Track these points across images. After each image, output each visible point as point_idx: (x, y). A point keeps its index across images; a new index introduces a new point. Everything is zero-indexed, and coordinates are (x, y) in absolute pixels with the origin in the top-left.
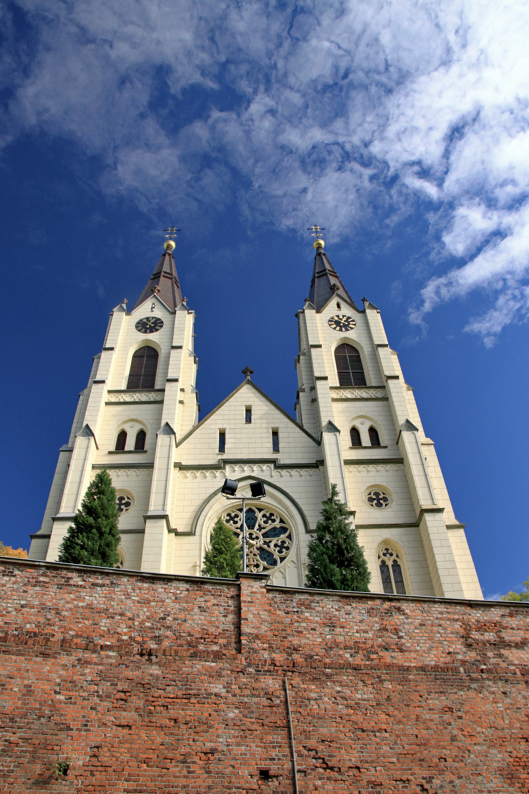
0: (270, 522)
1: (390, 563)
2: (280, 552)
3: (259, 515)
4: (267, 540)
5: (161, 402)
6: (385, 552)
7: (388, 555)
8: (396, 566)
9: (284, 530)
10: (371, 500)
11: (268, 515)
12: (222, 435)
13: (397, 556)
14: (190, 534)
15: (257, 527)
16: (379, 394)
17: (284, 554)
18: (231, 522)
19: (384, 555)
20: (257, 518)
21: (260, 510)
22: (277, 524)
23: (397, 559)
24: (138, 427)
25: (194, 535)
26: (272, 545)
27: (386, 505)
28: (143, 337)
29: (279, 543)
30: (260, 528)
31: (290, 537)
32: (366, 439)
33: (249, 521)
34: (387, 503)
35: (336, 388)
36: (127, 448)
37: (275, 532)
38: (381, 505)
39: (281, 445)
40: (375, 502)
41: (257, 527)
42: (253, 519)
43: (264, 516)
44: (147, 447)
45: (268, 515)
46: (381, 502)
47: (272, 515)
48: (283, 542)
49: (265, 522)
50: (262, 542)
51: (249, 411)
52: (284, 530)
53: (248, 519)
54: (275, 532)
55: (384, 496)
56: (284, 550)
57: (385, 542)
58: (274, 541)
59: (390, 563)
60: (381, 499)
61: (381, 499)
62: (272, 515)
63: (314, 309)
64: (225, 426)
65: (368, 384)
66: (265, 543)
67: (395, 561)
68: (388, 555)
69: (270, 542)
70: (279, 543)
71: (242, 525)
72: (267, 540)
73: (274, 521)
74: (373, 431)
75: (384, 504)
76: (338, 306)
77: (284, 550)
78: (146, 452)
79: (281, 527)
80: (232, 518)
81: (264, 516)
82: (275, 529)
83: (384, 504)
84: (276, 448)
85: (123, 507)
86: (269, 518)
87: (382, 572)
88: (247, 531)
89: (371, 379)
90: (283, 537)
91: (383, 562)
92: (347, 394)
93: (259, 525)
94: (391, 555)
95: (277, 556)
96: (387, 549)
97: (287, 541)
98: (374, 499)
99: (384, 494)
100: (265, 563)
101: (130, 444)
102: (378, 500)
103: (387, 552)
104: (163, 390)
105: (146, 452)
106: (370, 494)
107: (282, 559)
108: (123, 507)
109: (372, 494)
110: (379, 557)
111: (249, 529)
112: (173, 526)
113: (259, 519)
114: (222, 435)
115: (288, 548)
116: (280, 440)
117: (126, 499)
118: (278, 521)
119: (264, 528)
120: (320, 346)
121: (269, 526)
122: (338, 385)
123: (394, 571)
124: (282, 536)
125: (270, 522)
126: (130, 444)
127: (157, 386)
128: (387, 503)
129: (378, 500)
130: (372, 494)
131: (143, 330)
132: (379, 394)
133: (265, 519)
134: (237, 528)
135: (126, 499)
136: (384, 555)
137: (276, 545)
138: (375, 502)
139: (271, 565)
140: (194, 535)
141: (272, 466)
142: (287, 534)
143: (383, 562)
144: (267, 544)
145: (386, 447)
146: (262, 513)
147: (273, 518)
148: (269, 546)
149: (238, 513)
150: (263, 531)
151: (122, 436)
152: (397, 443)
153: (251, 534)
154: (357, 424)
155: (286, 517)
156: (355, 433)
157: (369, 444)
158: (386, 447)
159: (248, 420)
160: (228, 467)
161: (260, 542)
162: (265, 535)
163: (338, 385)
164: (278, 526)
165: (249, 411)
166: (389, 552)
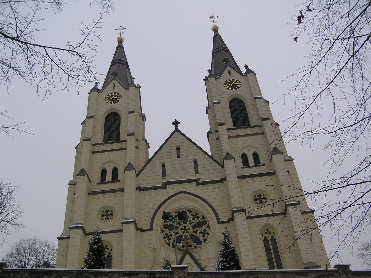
0: (196, 218)
1: (269, 238)
2: (203, 236)
4: (195, 230)
5: (125, 149)
6: (266, 231)
7: (268, 233)
8: (273, 240)
9: (205, 223)
10: (256, 200)
11: (195, 214)
12: (163, 166)
13: (274, 233)
14: (151, 229)
15: (188, 222)
16: (258, 130)
19: (266, 233)
20: (188, 216)
22: (201, 220)
23: (273, 235)
24: (113, 166)
25: (152, 230)
26: (198, 232)
29: (203, 231)
31: (208, 227)
34: (266, 201)
35: (231, 129)
37: (199, 225)
38: (263, 202)
39: (199, 170)
40: (259, 200)
43: (192, 215)
44: (119, 178)
45: (195, 214)
46: (263, 200)
47: (197, 214)
48: (205, 230)
49: (193, 219)
50: (192, 231)
51: (178, 149)
54: (199, 225)
55: (264, 196)
56: (206, 235)
57: (267, 225)
58: (200, 230)
59: (269, 238)
60: (262, 199)
61: (262, 199)
64: (164, 161)
65: (252, 125)
66: (194, 231)
67: (272, 237)
68: (268, 233)
69: (197, 231)
70: (203, 231)
72: (195, 230)
73: (198, 218)
74: (256, 156)
75: (264, 202)
77: (206, 235)
78: (119, 181)
79: (203, 221)
81: (192, 215)
82: (199, 222)
83: (264, 202)
84: (197, 171)
85: (109, 216)
87: (265, 244)
89: (253, 121)
90: (204, 227)
91: (265, 238)
92: (240, 132)
93: (190, 221)
94: (270, 233)
95: (201, 239)
96: (267, 230)
97: (207, 229)
98: (258, 199)
99: (264, 195)
102: (261, 199)
103: (267, 231)
104: (125, 141)
105: (119, 181)
106: (255, 196)
107: (205, 241)
108: (109, 216)
109: (257, 196)
110: (263, 235)
112: (139, 227)
113: (189, 217)
114: (163, 166)
115: (208, 234)
116: (199, 167)
118: (201, 217)
121: (196, 221)
122: (233, 127)
123: (272, 243)
125: (196, 218)
127: (122, 139)
128: (266, 201)
129: (261, 199)
130: (257, 196)
132: (258, 130)
136: (266, 233)
137: (201, 233)
138: (259, 200)
139: (199, 245)
140: (152, 230)
141: (195, 183)
142: (207, 225)
143: (265, 238)
144: (195, 232)
145: (264, 165)
146: (191, 213)
147: (198, 216)
148: (196, 233)
151: (104, 172)
152: (271, 162)
153: (185, 227)
154: (245, 151)
155: (206, 214)
156: (244, 157)
157: (253, 164)
158: (264, 165)
159: (179, 155)
160: (168, 186)
161: (191, 231)
162: (194, 227)
163: (233, 127)
165: (178, 149)
166: (269, 231)
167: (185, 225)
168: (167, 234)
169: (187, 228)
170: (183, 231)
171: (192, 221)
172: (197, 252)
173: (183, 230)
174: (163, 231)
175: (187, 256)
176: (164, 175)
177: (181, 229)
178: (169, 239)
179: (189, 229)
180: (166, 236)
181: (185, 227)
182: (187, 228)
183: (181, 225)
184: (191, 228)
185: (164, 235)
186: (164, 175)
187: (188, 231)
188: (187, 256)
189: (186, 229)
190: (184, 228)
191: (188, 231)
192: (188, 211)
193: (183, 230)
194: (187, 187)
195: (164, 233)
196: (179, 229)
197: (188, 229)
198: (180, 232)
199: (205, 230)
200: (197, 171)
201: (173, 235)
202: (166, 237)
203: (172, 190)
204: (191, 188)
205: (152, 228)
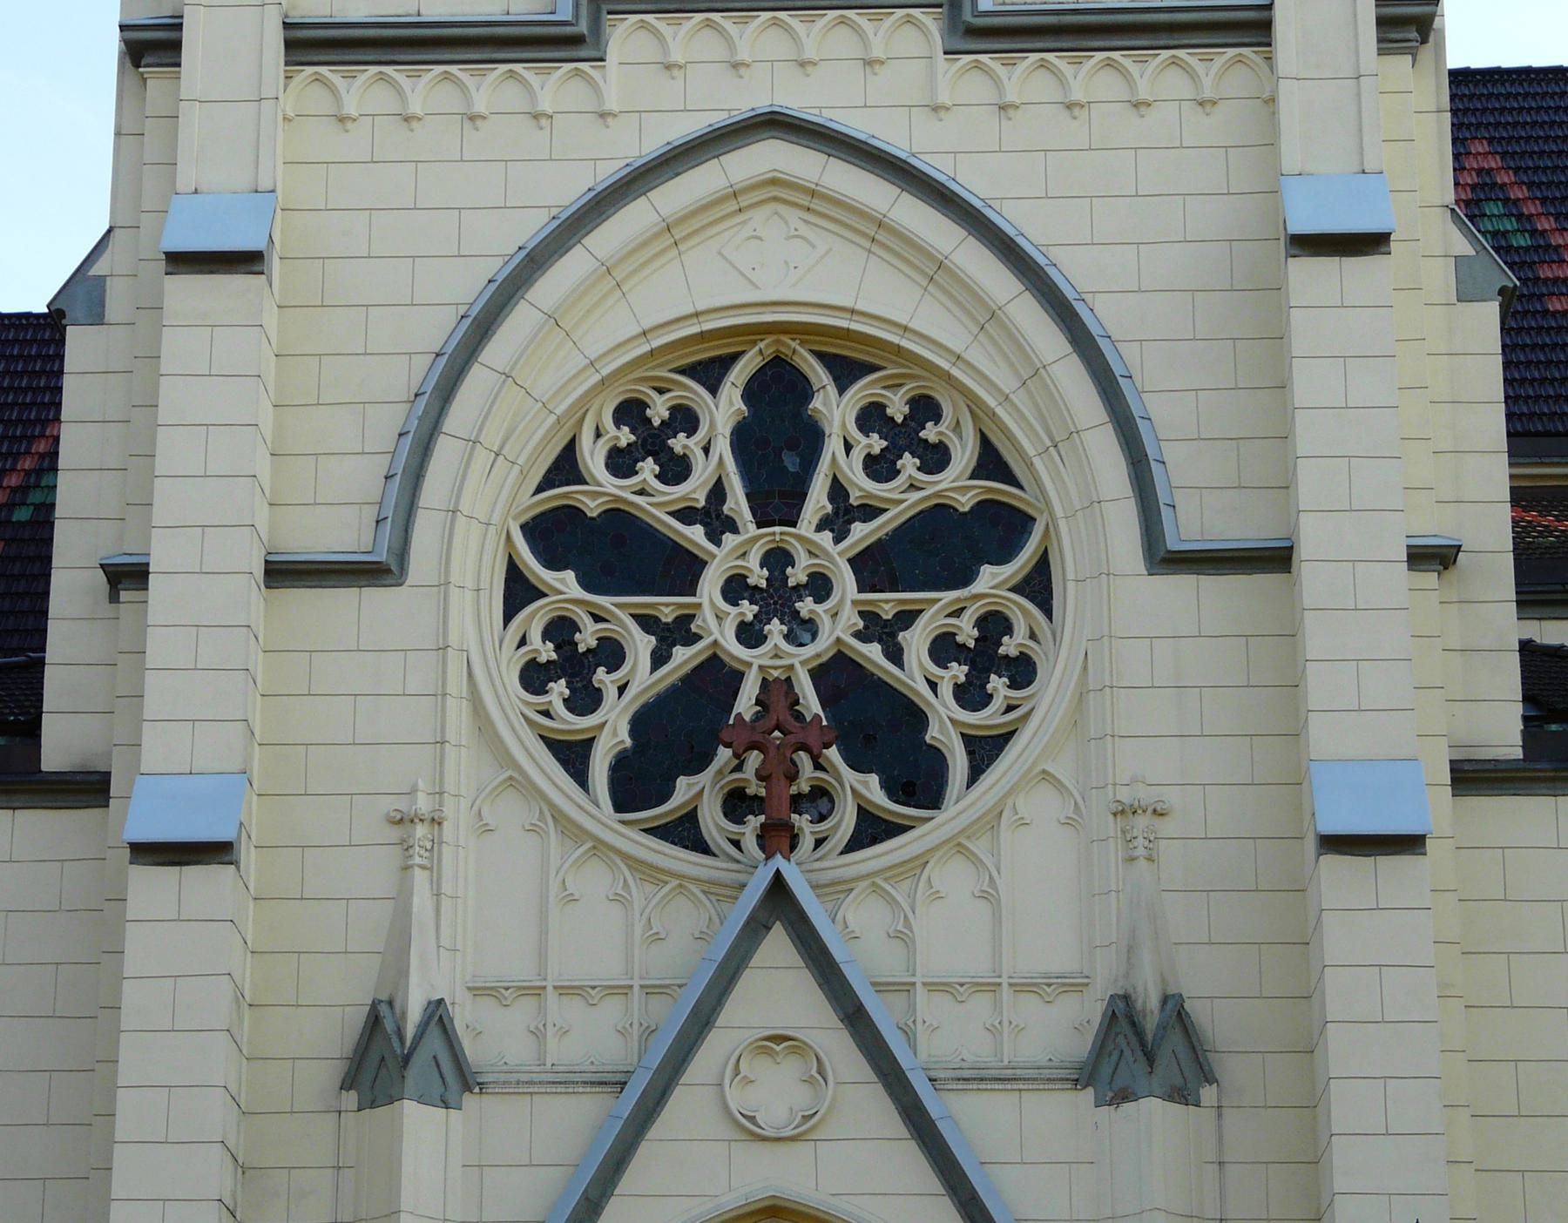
0: (908, 463)
2: (971, 695)
3: (835, 410)
4: (888, 603)
11: (898, 409)
15: (817, 501)
21: (846, 371)
22: (957, 485)
26: (916, 641)
29: (967, 633)
30: (843, 513)
45: (898, 409)
47: (924, 408)
48: (994, 625)
49: (881, 467)
50: (851, 619)
62: (924, 408)
73: (935, 459)
77: (997, 684)
81: (871, 418)
82: (938, 515)
86: (904, 436)
93: (838, 491)
95: (946, 724)
97: (1022, 612)
119: (869, 512)
125: (908, 464)
133: (877, 444)
137: (944, 648)
146: (862, 391)
149: (693, 392)
150: (862, 533)
161: (838, 621)
162: (874, 568)
164: (965, 503)
168: (560, 630)
171: (861, 486)
174: (519, 591)
178: (585, 700)
181: (778, 559)
192: (825, 359)
195: (535, 618)
196: (710, 585)
199: (994, 625)
201: (641, 645)
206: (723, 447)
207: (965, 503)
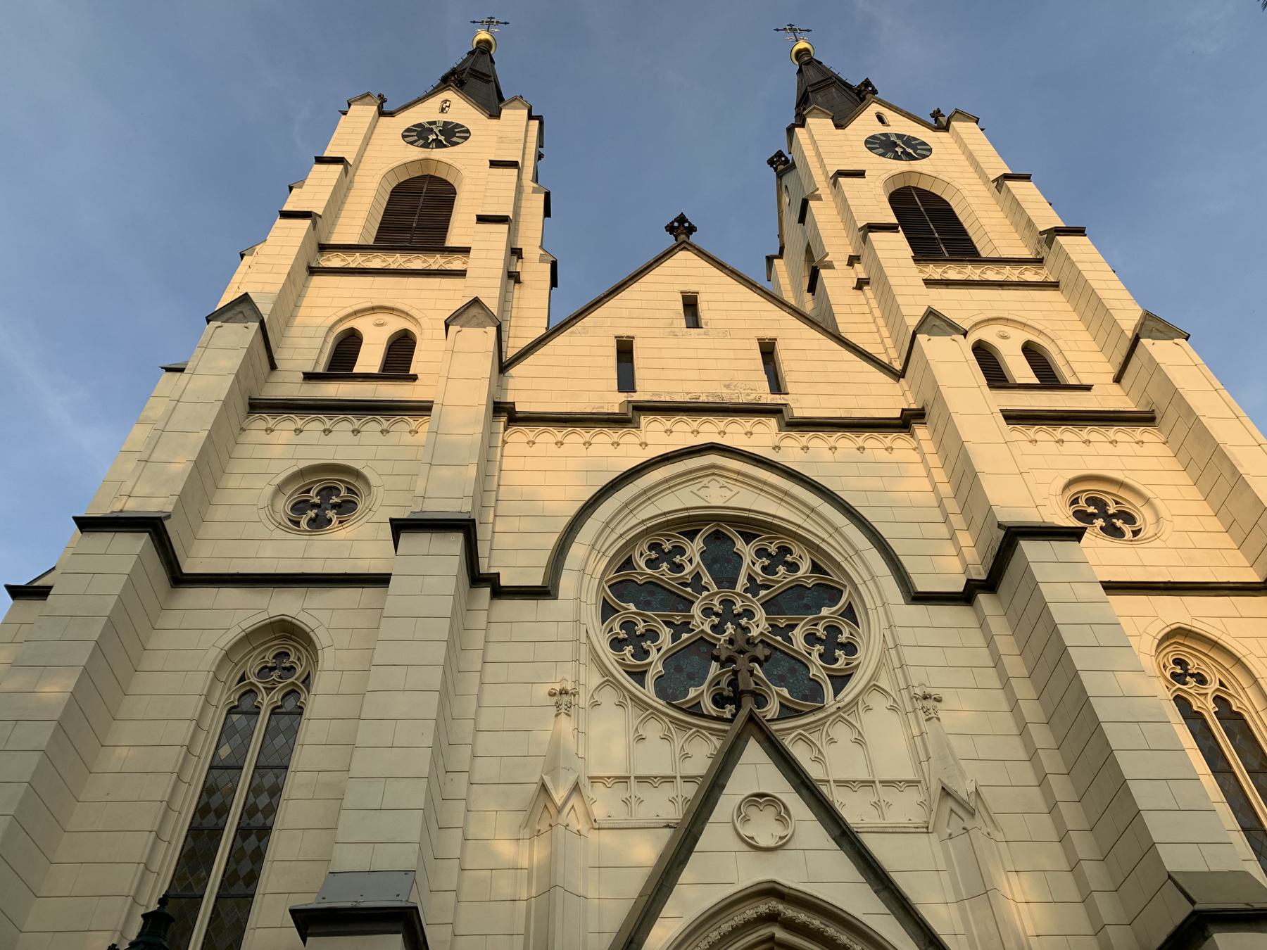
1: (1207, 708)
2: (828, 657)
3: (747, 551)
15: (742, 581)
17: (840, 664)
18: (665, 566)
24: (395, 324)
26: (798, 635)
27: (1135, 533)
28: (416, 153)
29: (821, 632)
30: (753, 587)
31: (849, 613)
32: (1021, 370)
33: (716, 567)
36: (357, 369)
41: (742, 581)
42: (728, 561)
43: (761, 552)
47: (785, 550)
52: (833, 593)
53: (715, 561)
59: (1207, 708)
63: (827, 115)
69: (792, 627)
70: (821, 632)
71: (697, 577)
76: (880, 118)
78: (414, 378)
80: (667, 556)
82: (798, 588)
83: (1127, 529)
84: (776, 385)
88: (712, 594)
93: (751, 579)
95: (817, 669)
100: (785, 692)
101: (370, 358)
105: (414, 378)
107: (840, 681)
111: (719, 585)
113: (747, 560)
115: (850, 649)
117: (343, 493)
118: (805, 566)
120: (860, 174)
124: (825, 611)
126: (370, 358)
127: (453, 240)
131: (421, 142)
134: (685, 585)
135: (343, 493)
137: (811, 639)
139: (805, 698)
141: (773, 422)
146: (755, 544)
148: (790, 640)
153: (728, 603)
164: (810, 583)
167: (727, 592)
168: (628, 625)
169: (738, 608)
170: (717, 620)
172: (801, 738)
173: (717, 614)
174: (607, 611)
175: (753, 751)
176: (626, 381)
177: (707, 611)
179: (749, 614)
180: (623, 635)
181: (728, 603)
182: (738, 608)
183: (705, 593)
184: (760, 614)
185: (611, 630)
186: (626, 381)
187: (744, 621)
188: (753, 751)
189: (728, 614)
190: (718, 608)
191: (744, 621)
193: (717, 614)
194: (735, 433)
196: (696, 610)
197: (739, 615)
198: (703, 625)
199: (833, 630)
200: (776, 385)
201: (666, 634)
202: (624, 640)
203: (659, 436)
204: (760, 436)
205: (556, 587)
206: (697, 559)
207: (810, 583)
